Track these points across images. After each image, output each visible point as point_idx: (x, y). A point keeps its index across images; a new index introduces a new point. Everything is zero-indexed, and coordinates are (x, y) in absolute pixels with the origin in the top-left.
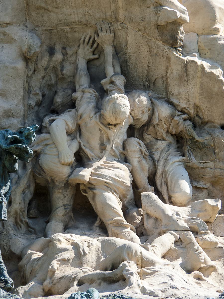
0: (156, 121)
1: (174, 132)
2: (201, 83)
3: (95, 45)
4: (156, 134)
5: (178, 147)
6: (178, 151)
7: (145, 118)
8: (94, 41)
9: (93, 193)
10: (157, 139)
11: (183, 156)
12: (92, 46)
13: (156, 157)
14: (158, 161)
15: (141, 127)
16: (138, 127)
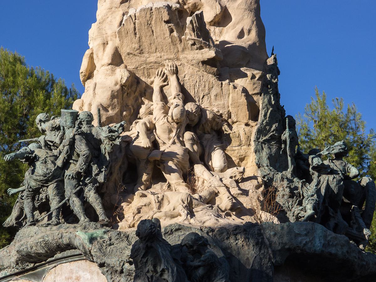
0: (203, 121)
1: (216, 128)
2: (232, 97)
3: (165, 76)
4: (204, 130)
5: (219, 138)
6: (218, 141)
7: (196, 120)
8: (164, 74)
9: (164, 166)
10: (205, 133)
11: (222, 143)
12: (163, 77)
13: (205, 143)
14: (206, 147)
15: (194, 126)
16: (193, 125)
